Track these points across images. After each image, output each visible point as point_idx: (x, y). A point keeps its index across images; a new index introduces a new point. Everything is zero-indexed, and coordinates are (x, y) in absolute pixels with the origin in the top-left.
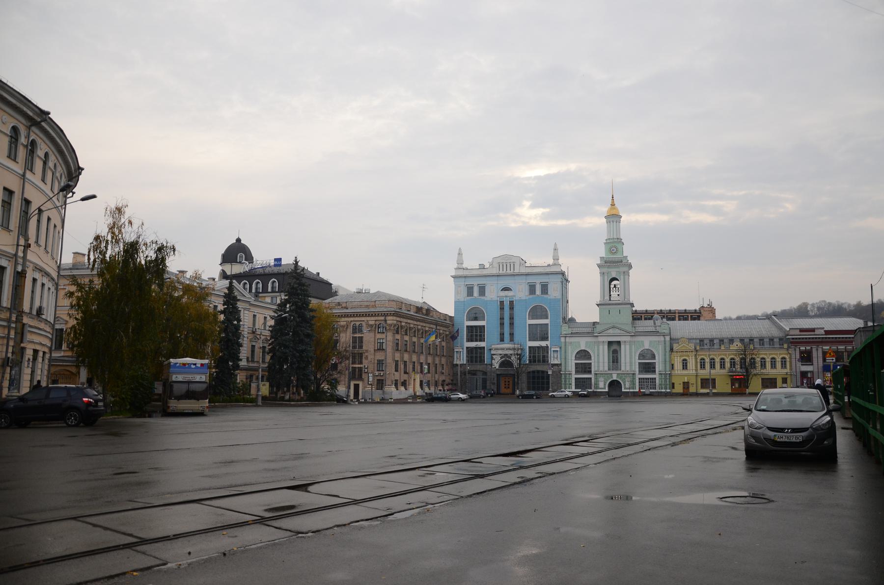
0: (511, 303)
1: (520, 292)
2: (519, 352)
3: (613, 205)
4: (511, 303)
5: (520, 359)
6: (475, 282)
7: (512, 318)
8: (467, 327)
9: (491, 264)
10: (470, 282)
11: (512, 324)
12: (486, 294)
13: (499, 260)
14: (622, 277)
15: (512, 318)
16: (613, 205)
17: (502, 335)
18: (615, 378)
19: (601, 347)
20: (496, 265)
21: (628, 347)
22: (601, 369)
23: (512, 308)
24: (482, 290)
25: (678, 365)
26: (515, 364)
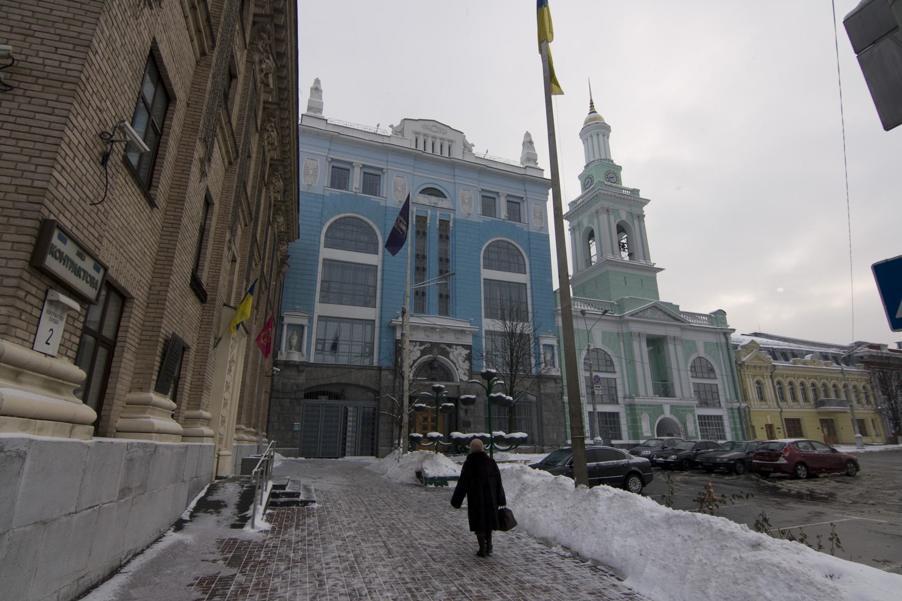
0: (444, 224)
1: (464, 204)
2: (468, 341)
3: (593, 111)
4: (444, 224)
5: (469, 358)
6: (358, 160)
7: (444, 260)
8: (324, 260)
9: (399, 131)
10: (343, 155)
11: (443, 272)
12: (384, 191)
13: (418, 127)
14: (636, 222)
15: (444, 260)
16: (593, 111)
17: (420, 295)
18: (667, 414)
19: (636, 344)
20: (409, 135)
21: (679, 348)
22: (642, 391)
23: (444, 237)
24: (372, 182)
25: (752, 393)
26: (461, 374)
